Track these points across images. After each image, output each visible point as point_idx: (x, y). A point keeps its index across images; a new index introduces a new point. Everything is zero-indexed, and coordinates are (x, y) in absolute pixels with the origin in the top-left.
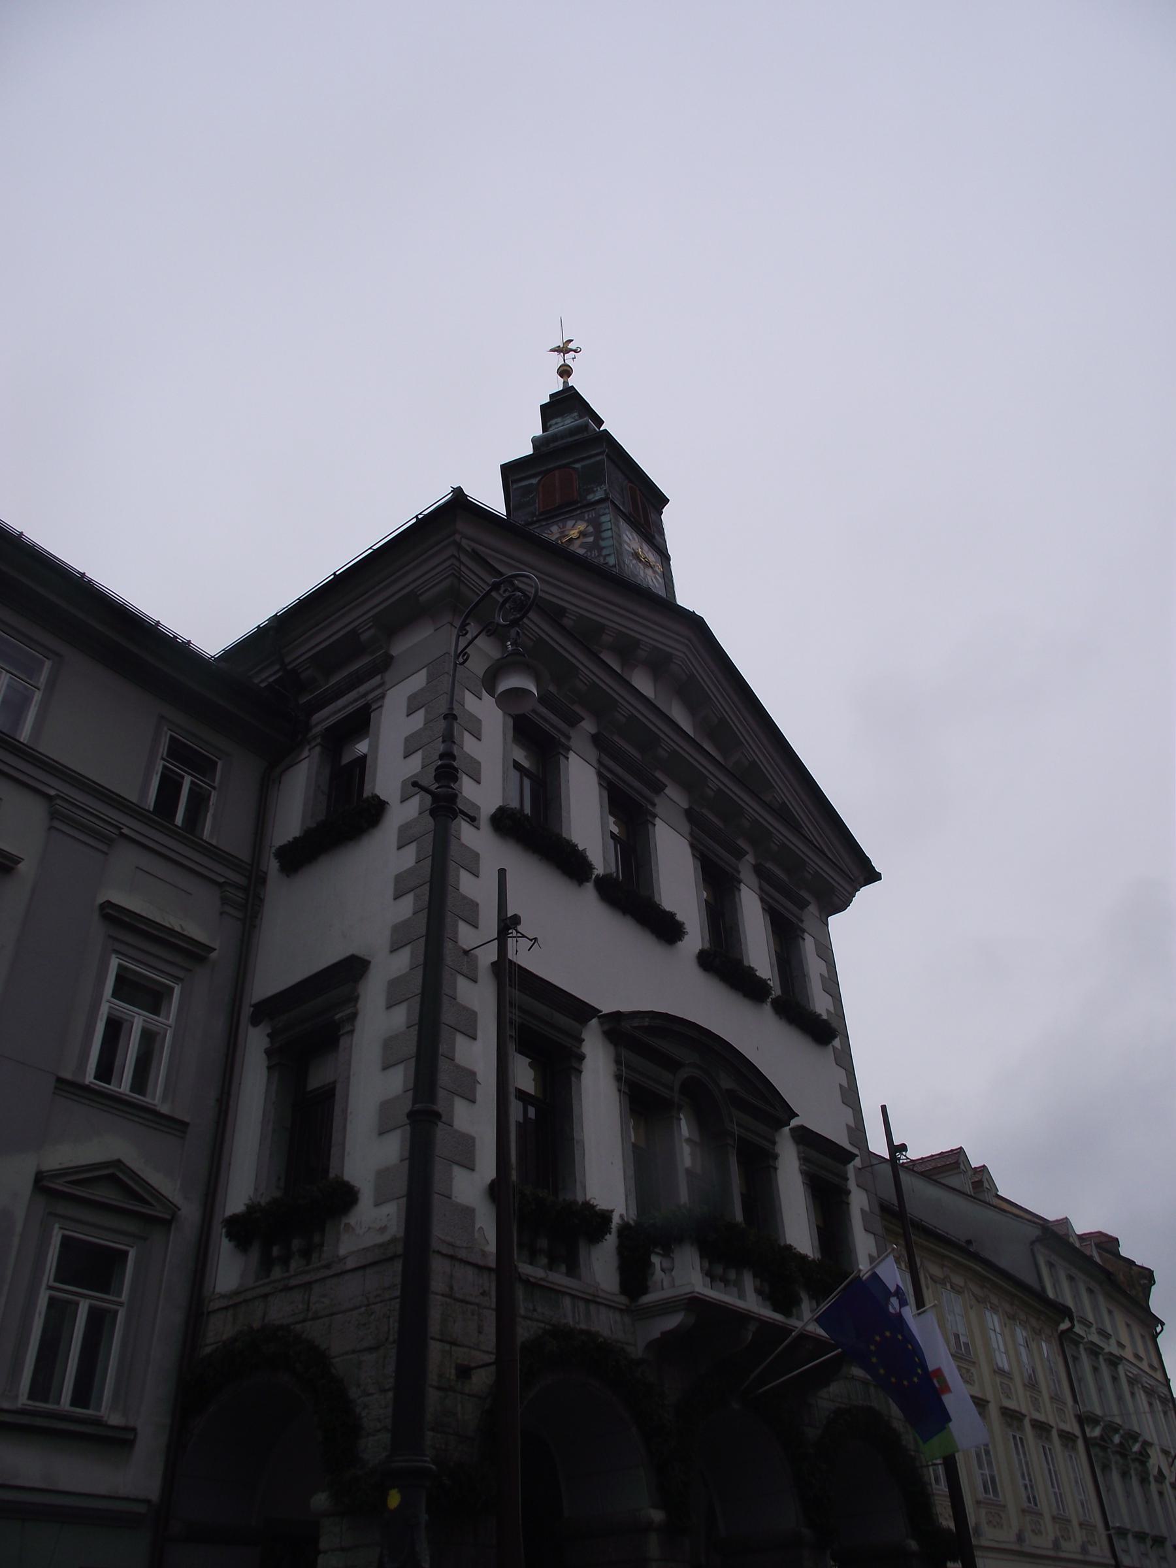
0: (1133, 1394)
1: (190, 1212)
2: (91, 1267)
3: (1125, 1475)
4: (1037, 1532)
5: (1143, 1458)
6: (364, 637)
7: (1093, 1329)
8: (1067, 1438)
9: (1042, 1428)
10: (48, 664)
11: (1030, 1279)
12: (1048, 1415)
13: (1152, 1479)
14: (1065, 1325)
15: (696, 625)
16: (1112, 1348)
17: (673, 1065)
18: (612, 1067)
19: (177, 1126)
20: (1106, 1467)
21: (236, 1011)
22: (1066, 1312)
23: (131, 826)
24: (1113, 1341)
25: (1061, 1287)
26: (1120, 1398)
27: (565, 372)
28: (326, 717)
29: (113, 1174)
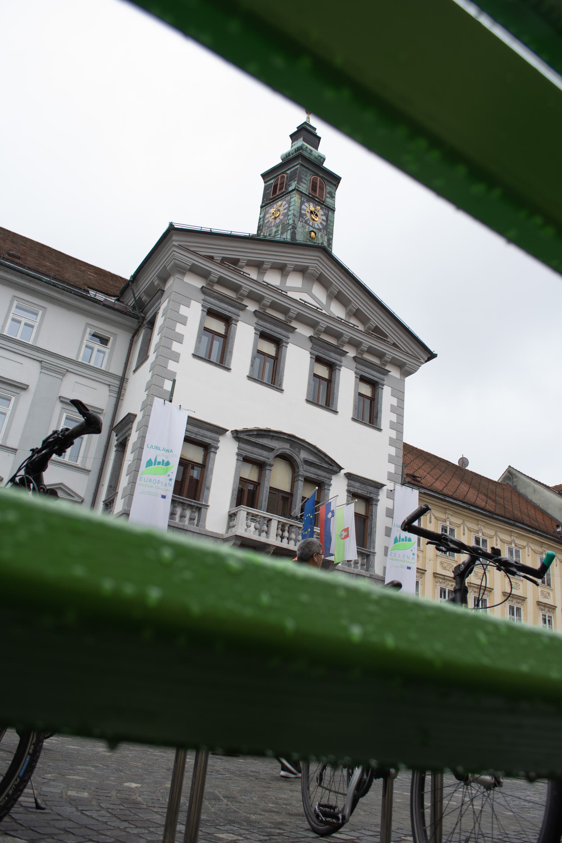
6: (155, 284)
10: (40, 312)
17: (271, 450)
18: (236, 451)
19: (87, 471)
28: (149, 316)
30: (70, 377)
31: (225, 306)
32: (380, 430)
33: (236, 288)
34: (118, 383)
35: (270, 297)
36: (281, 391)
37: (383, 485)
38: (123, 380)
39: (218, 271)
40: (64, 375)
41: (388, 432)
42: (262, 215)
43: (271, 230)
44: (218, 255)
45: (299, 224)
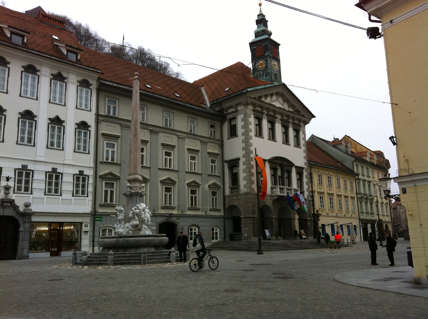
0: (374, 187)
1: (222, 186)
2: (214, 194)
3: (366, 203)
4: (341, 213)
5: (372, 199)
7: (366, 176)
8: (352, 198)
9: (346, 197)
11: (351, 168)
12: (349, 194)
13: (374, 203)
14: (357, 177)
15: (284, 85)
16: (371, 179)
17: (277, 163)
20: (361, 202)
21: (223, 161)
22: (358, 175)
23: (207, 140)
24: (371, 178)
25: (358, 169)
26: (370, 189)
27: (260, 5)
28: (229, 117)
29: (215, 184)
30: (209, 144)
31: (259, 114)
32: (301, 148)
33: (262, 107)
34: (220, 143)
35: (272, 108)
36: (276, 141)
37: (304, 168)
38: (222, 141)
39: (258, 103)
40: (206, 143)
41: (303, 148)
42: (253, 64)
43: (260, 73)
44: (257, 96)
45: (272, 71)
